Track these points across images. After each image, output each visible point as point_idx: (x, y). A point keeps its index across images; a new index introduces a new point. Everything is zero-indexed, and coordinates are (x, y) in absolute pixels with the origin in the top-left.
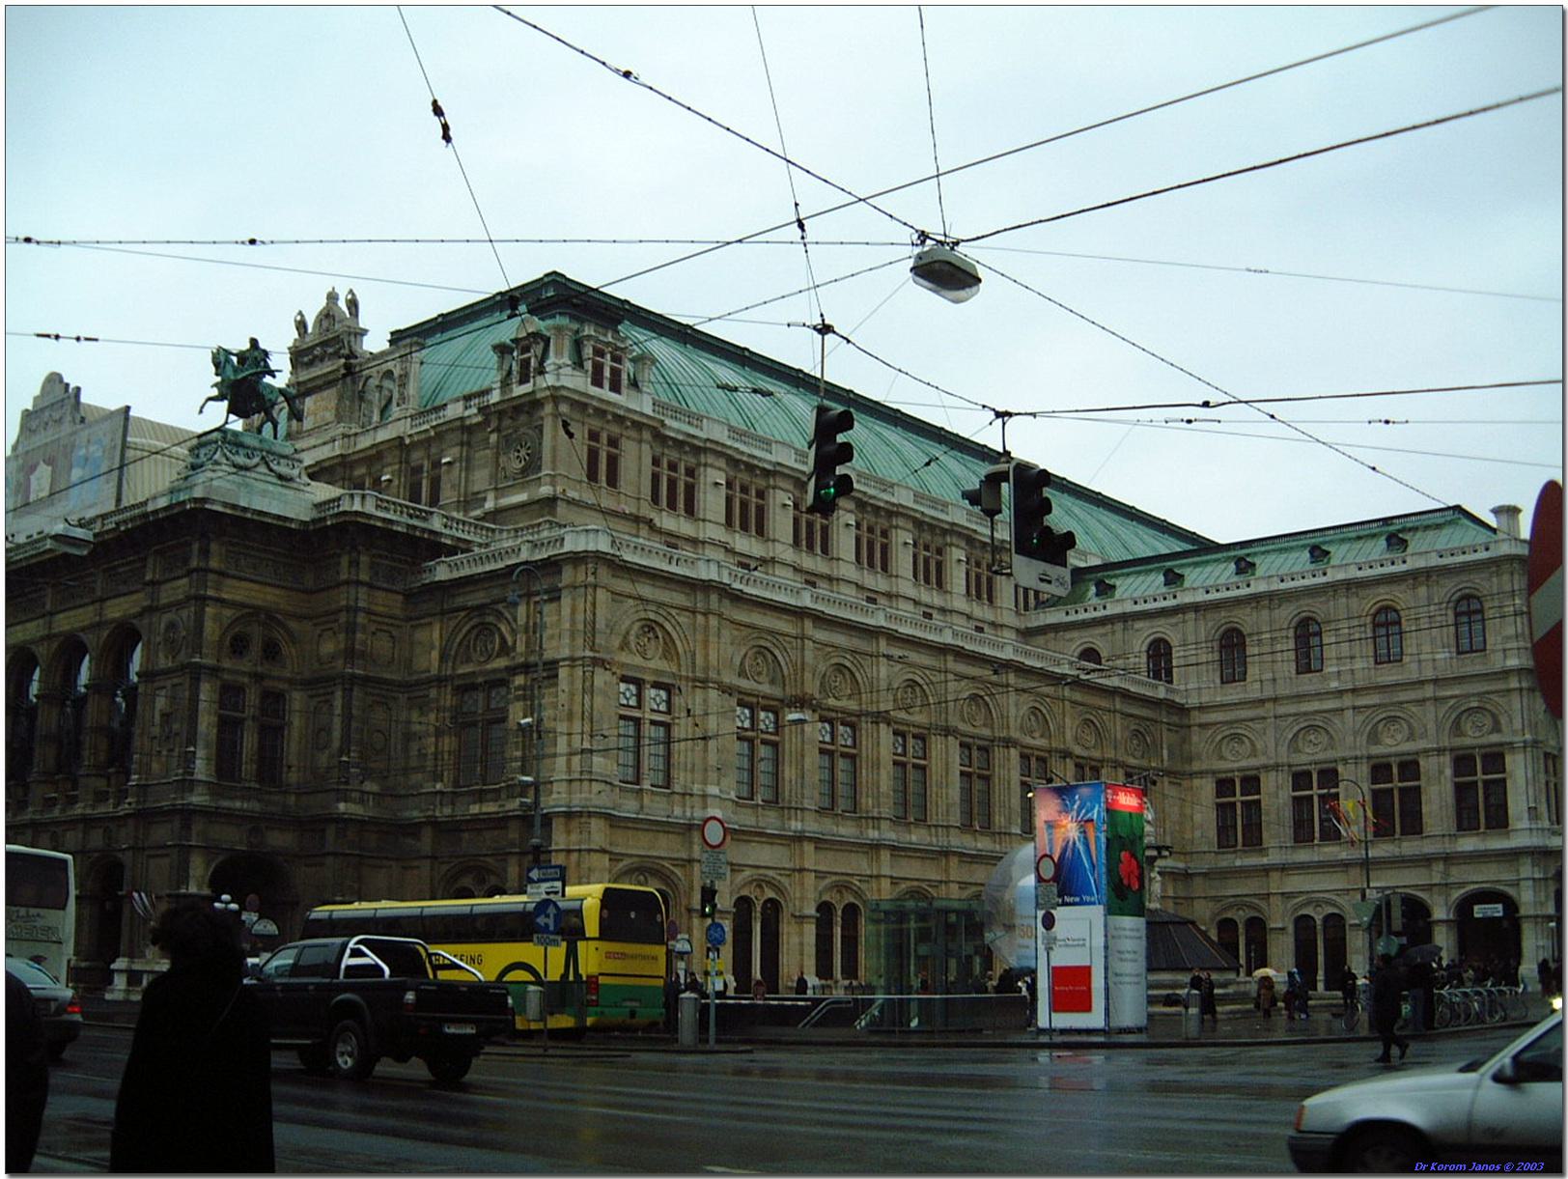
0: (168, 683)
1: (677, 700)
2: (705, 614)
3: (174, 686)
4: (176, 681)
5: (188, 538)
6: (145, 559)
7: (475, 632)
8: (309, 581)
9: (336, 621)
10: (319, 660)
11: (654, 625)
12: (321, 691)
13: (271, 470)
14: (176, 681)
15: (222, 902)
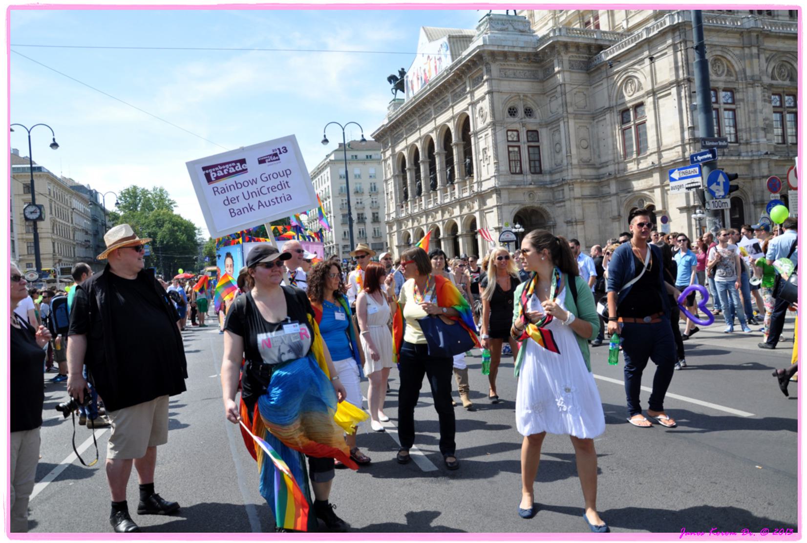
0: (483, 135)
1: (738, 96)
2: (749, 47)
3: (486, 135)
4: (486, 133)
5: (481, 67)
6: (465, 83)
7: (626, 81)
8: (541, 74)
9: (556, 91)
10: (551, 112)
11: (720, 57)
12: (554, 126)
13: (515, 29)
14: (486, 133)
15: (516, 228)
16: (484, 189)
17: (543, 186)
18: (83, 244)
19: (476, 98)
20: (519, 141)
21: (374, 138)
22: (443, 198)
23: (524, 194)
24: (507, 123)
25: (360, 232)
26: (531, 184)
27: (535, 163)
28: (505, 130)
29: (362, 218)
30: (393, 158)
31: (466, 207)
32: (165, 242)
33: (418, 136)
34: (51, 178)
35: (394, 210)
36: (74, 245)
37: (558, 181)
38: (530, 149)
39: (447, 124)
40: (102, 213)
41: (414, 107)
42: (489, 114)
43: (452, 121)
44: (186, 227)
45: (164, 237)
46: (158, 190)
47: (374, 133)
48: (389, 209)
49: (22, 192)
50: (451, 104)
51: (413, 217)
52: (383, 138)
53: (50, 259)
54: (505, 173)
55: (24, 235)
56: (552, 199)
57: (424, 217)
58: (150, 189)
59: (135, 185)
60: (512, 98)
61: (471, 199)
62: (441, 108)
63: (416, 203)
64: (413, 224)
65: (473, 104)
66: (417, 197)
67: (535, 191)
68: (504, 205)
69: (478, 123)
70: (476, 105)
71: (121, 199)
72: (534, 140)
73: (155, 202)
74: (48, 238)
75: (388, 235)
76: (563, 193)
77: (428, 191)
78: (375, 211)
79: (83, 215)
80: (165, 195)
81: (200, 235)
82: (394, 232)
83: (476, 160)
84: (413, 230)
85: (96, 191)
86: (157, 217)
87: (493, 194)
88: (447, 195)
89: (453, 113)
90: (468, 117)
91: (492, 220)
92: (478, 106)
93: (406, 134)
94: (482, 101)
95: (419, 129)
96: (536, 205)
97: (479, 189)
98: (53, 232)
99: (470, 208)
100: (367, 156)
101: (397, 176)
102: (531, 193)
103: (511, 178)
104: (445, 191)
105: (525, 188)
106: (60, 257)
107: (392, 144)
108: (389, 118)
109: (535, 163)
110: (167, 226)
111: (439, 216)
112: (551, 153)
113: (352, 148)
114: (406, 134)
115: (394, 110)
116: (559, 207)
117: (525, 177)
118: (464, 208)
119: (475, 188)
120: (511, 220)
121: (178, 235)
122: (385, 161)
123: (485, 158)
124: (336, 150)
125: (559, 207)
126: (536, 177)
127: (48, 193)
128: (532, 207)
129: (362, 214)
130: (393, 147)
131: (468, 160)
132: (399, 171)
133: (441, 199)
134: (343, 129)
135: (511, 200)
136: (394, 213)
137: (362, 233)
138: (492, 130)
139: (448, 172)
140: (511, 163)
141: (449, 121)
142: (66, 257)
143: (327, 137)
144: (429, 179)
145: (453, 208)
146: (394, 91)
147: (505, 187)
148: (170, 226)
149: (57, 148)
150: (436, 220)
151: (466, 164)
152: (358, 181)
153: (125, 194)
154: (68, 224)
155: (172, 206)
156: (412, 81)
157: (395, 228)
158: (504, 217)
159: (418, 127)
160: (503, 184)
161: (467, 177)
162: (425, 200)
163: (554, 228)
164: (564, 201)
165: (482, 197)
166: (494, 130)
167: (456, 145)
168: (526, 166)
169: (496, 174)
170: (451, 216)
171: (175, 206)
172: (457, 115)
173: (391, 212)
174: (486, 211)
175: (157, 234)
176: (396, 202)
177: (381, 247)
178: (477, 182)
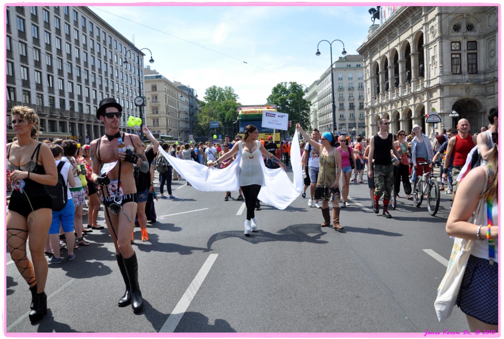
0: (433, 46)
3: (435, 46)
4: (435, 45)
14: (435, 45)
15: (453, 114)
16: (431, 85)
17: (478, 83)
18: (184, 120)
19: (429, 20)
20: (460, 49)
21: (358, 52)
22: (403, 92)
23: (462, 89)
24: (452, 37)
25: (351, 115)
26: (468, 82)
27: (472, 67)
28: (450, 42)
29: (353, 106)
30: (370, 66)
31: (418, 99)
32: (230, 120)
33: (388, 49)
34: (167, 82)
35: (370, 101)
36: (179, 121)
37: (490, 79)
38: (469, 55)
39: (408, 40)
40: (196, 102)
41: (385, 29)
42: (437, 31)
43: (411, 38)
46: (228, 88)
47: (358, 49)
48: (367, 100)
49: (151, 90)
50: (410, 25)
51: (382, 106)
52: (364, 51)
53: (164, 129)
54: (448, 74)
56: (484, 92)
57: (390, 105)
58: (223, 88)
59: (214, 85)
60: (456, 18)
61: (422, 93)
62: (404, 29)
63: (385, 96)
64: (382, 110)
65: (426, 24)
66: (385, 92)
67: (471, 87)
68: (446, 97)
69: (429, 38)
70: (429, 25)
71: (206, 94)
72: (473, 48)
73: (226, 95)
74: (164, 116)
76: (494, 88)
77: (393, 88)
78: (361, 102)
80: (232, 91)
83: (427, 65)
84: (382, 114)
85: (193, 89)
87: (438, 89)
88: (406, 90)
89: (412, 32)
90: (422, 34)
91: (437, 107)
92: (430, 26)
93: (380, 49)
94: (433, 21)
95: (389, 44)
96: (471, 97)
97: (428, 86)
99: (421, 99)
100: (357, 65)
101: (373, 77)
102: (467, 88)
103: (451, 77)
104: (404, 87)
105: (462, 85)
106: (170, 128)
107: (370, 56)
108: (368, 38)
109: (472, 67)
110: (231, 109)
112: (486, 57)
113: (348, 60)
114: (380, 48)
115: (372, 32)
116: (489, 98)
117: (464, 76)
118: (417, 99)
119: (425, 86)
120: (451, 108)
122: (366, 67)
123: (433, 63)
124: (337, 62)
125: (489, 98)
126: (472, 76)
127: (164, 90)
128: (468, 98)
129: (353, 103)
130: (371, 58)
131: (421, 65)
132: (374, 74)
133: (401, 93)
134: (331, 45)
135: (451, 93)
136: (370, 103)
137: (352, 116)
138: (439, 42)
139: (407, 74)
140: (453, 66)
141: (409, 38)
142: (174, 128)
143: (320, 51)
144: (394, 79)
145: (409, 99)
146: (373, 19)
147: (447, 84)
149: (153, 62)
150: (397, 108)
151: (419, 68)
152: (351, 81)
153: (209, 90)
154: (176, 109)
155: (236, 97)
156: (385, 11)
157: (370, 113)
158: (445, 106)
159: (388, 43)
160: (446, 82)
161: (420, 78)
162: (391, 94)
163: (484, 114)
164: (494, 94)
165: (430, 91)
166: (441, 42)
167: (414, 54)
168: (465, 68)
169: (441, 75)
170: (407, 105)
171: (238, 98)
172: (415, 33)
173: (368, 102)
174: (432, 102)
176: (372, 95)
178: (427, 81)
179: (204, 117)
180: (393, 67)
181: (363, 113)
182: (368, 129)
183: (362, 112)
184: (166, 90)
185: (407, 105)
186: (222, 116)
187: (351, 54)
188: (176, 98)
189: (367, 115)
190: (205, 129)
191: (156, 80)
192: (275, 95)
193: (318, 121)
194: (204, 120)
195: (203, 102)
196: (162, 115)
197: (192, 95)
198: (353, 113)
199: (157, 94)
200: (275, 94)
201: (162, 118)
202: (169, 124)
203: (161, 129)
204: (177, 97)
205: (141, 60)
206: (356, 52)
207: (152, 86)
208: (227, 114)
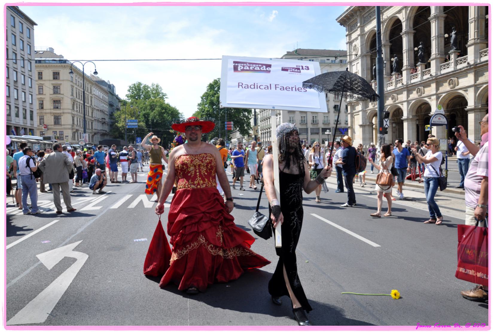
21: (338, 22)
25: (302, 120)
32: (155, 121)
40: (117, 101)
44: (172, 112)
45: (155, 117)
46: (155, 86)
47: (341, 16)
49: (52, 78)
53: (69, 129)
55: (52, 110)
57: (405, 93)
58: (150, 85)
71: (129, 91)
74: (69, 113)
75: (349, 116)
79: (103, 100)
80: (160, 90)
81: (181, 118)
82: (358, 112)
86: (152, 103)
98: (73, 109)
101: (366, 56)
106: (77, 128)
107: (361, 24)
111: (432, 89)
121: (165, 117)
127: (70, 79)
130: (362, 27)
139: (453, 36)
145: (458, 78)
148: (160, 109)
150: (423, 95)
153: (132, 88)
162: (407, 75)
171: (166, 98)
175: (149, 115)
177: (317, 132)
179: (123, 116)
180: (410, 33)
181: (316, 116)
182: (353, 132)
183: (314, 116)
184: (76, 82)
185: (454, 87)
186: (146, 116)
187: (302, 48)
188: (89, 92)
189: (351, 111)
190: (123, 131)
191: (59, 66)
192: (211, 93)
193: (259, 126)
194: (122, 120)
195: (125, 100)
196: (66, 111)
197: (112, 92)
198: (304, 117)
199: (61, 84)
200: (211, 91)
201: (65, 115)
202: (76, 123)
203: (65, 129)
204: (89, 91)
205: (29, 30)
206: (336, 21)
207: (54, 73)
208: (152, 114)
